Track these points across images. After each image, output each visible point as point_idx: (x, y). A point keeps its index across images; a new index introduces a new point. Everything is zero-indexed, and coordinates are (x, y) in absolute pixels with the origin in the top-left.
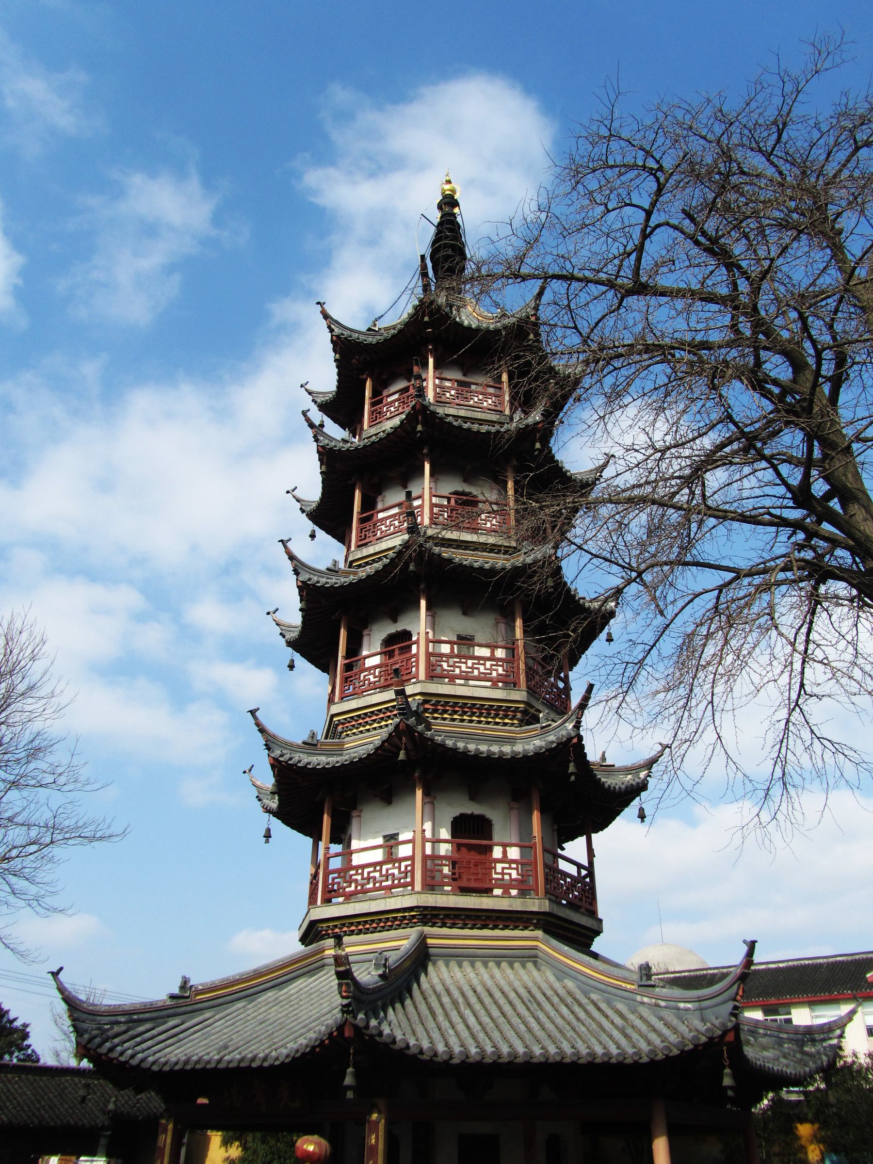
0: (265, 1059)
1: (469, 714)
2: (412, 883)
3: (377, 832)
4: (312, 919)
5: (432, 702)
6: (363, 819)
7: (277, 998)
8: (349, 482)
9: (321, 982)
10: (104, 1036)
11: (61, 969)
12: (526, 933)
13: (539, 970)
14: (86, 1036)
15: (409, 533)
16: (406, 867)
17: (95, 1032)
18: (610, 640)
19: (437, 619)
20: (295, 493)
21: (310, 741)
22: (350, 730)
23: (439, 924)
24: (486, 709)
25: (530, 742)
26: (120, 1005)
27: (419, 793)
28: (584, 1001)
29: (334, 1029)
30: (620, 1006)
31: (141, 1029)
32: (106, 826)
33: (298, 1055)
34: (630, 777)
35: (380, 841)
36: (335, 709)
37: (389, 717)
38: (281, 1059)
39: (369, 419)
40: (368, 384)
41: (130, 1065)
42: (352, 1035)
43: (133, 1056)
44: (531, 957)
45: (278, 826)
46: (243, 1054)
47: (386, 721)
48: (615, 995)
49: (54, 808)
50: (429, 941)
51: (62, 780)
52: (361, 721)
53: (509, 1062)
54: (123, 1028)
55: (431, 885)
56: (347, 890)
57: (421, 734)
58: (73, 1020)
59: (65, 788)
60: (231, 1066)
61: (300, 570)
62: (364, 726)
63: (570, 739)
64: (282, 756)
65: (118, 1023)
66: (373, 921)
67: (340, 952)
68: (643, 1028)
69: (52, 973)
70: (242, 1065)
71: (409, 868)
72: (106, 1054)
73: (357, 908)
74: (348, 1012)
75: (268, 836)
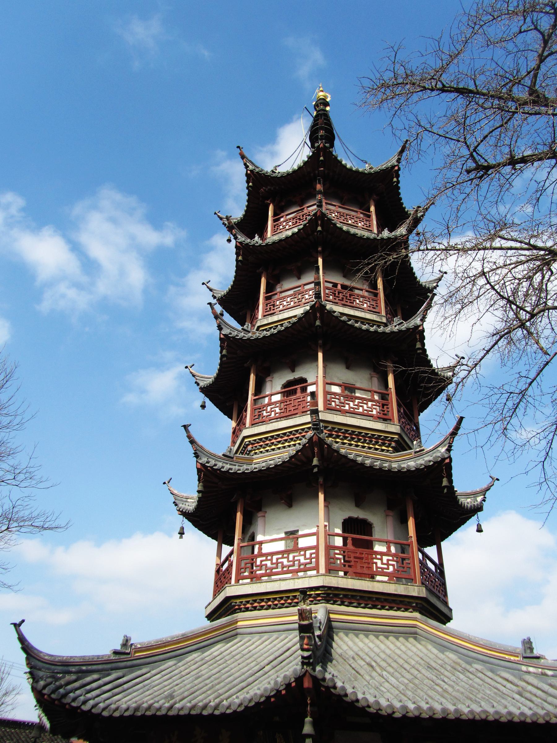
0: (216, 707)
1: (356, 440)
2: (317, 568)
3: (279, 529)
4: (228, 595)
5: (329, 428)
6: (266, 519)
7: (202, 659)
8: (258, 271)
9: (238, 648)
10: (57, 683)
11: (23, 621)
12: (406, 614)
13: (420, 644)
14: (42, 683)
16: (311, 554)
17: (49, 680)
19: (328, 370)
21: (228, 454)
22: (258, 449)
23: (339, 603)
24: (369, 437)
25: (408, 462)
26: (71, 657)
27: (321, 496)
28: (471, 670)
29: (293, 680)
30: (507, 675)
31: (88, 679)
32: (54, 519)
33: (252, 704)
34: (469, 500)
35: (283, 535)
37: (292, 439)
38: (233, 708)
39: (272, 230)
40: (271, 208)
41: (82, 710)
42: (311, 686)
43: (85, 702)
44: (411, 633)
45: (188, 526)
46: (193, 702)
47: (289, 442)
48: (498, 665)
49: (14, 500)
50: (332, 616)
51: (22, 477)
52: (268, 442)
53: (443, 718)
54: (73, 677)
55: (331, 570)
56: (258, 572)
57: (329, 446)
58: (31, 668)
59: (23, 485)
60: (182, 713)
61: (223, 326)
62: (270, 446)
63: (443, 459)
64: (208, 462)
65: (70, 672)
68: (539, 693)
69: (15, 625)
70: (193, 712)
71: (314, 556)
72: (59, 700)
73: (268, 587)
74: (308, 664)
75: (182, 533)
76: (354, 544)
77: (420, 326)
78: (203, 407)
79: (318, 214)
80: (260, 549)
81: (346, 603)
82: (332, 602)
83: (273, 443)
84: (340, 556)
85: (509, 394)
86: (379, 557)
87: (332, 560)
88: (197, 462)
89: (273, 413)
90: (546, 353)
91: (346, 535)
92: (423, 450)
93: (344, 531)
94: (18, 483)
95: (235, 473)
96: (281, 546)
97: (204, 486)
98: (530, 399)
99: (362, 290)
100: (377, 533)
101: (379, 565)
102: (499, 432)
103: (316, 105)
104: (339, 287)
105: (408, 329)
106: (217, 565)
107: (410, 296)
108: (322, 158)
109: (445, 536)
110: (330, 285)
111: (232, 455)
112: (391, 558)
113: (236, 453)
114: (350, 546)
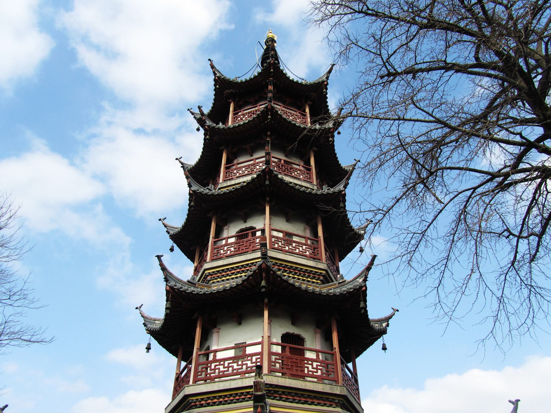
1: (293, 273)
3: (231, 342)
4: (186, 394)
6: (220, 334)
8: (220, 148)
11: (7, 406)
15: (266, 164)
16: (257, 359)
18: (361, 250)
19: (272, 222)
20: (181, 160)
21: (192, 281)
22: (216, 279)
23: (278, 398)
24: (303, 272)
32: (41, 332)
34: (377, 325)
36: (206, 266)
45: (155, 343)
47: (241, 273)
57: (274, 272)
59: (16, 304)
62: (225, 277)
63: (361, 287)
66: (231, 395)
67: (259, 380)
73: (220, 386)
75: (148, 348)
76: (290, 352)
77: (343, 191)
78: (172, 250)
79: (269, 107)
80: (215, 356)
81: (284, 399)
82: (272, 397)
83: (228, 275)
84: (280, 361)
85: (412, 234)
86: (310, 362)
87: (273, 364)
88: (167, 285)
89: (229, 252)
90: (440, 202)
91: (285, 344)
92: (345, 281)
93: (282, 341)
94: (12, 302)
95: (198, 294)
96: (231, 353)
97: (171, 305)
98: (428, 239)
99: (299, 165)
100: (308, 344)
101: (310, 369)
102: (405, 264)
103: (267, 42)
104: (282, 162)
105: (334, 193)
106: (177, 374)
107: (333, 172)
108: (272, 70)
109: (358, 355)
110: (276, 160)
111: (195, 282)
112: (319, 364)
113: (199, 281)
114: (288, 353)
